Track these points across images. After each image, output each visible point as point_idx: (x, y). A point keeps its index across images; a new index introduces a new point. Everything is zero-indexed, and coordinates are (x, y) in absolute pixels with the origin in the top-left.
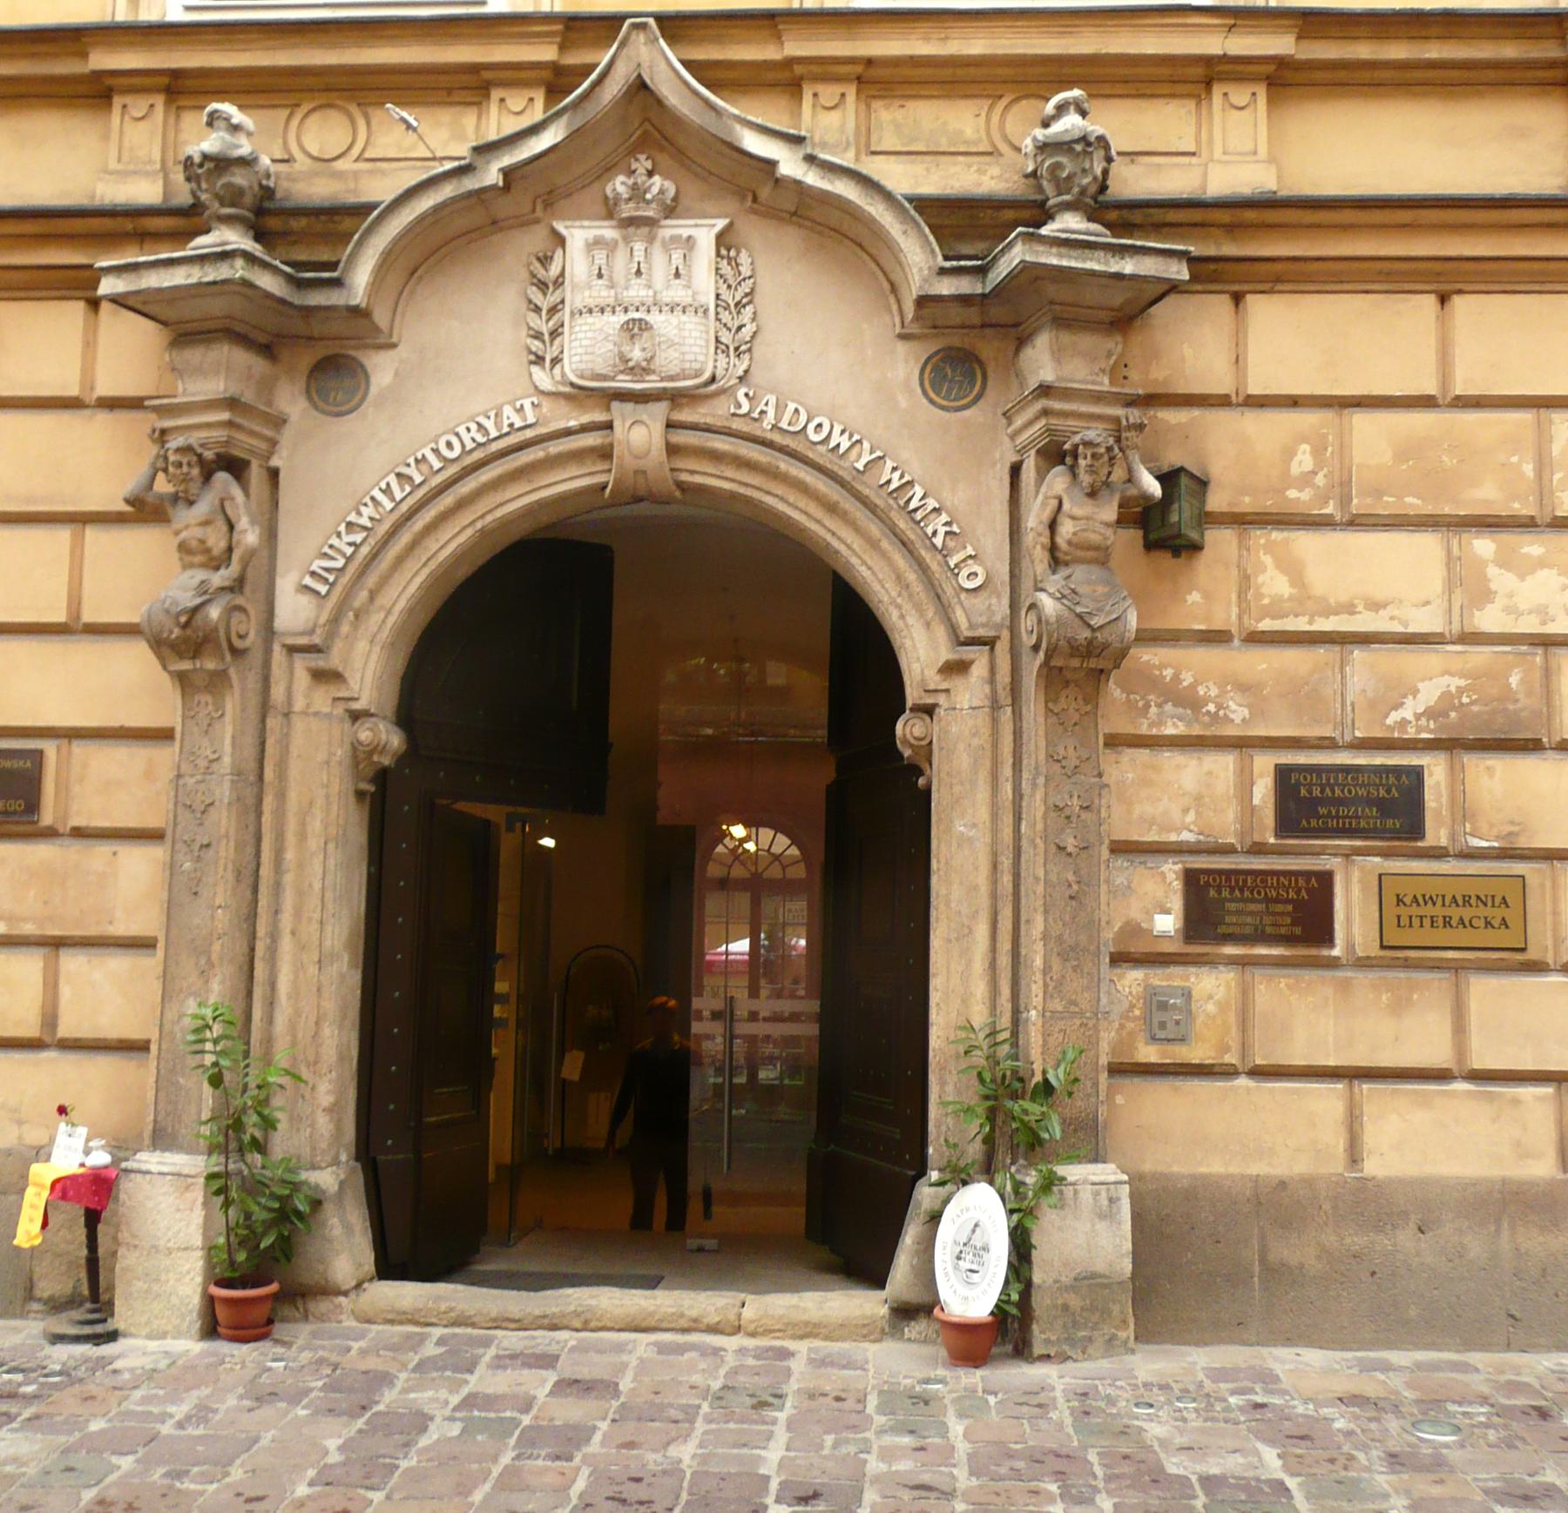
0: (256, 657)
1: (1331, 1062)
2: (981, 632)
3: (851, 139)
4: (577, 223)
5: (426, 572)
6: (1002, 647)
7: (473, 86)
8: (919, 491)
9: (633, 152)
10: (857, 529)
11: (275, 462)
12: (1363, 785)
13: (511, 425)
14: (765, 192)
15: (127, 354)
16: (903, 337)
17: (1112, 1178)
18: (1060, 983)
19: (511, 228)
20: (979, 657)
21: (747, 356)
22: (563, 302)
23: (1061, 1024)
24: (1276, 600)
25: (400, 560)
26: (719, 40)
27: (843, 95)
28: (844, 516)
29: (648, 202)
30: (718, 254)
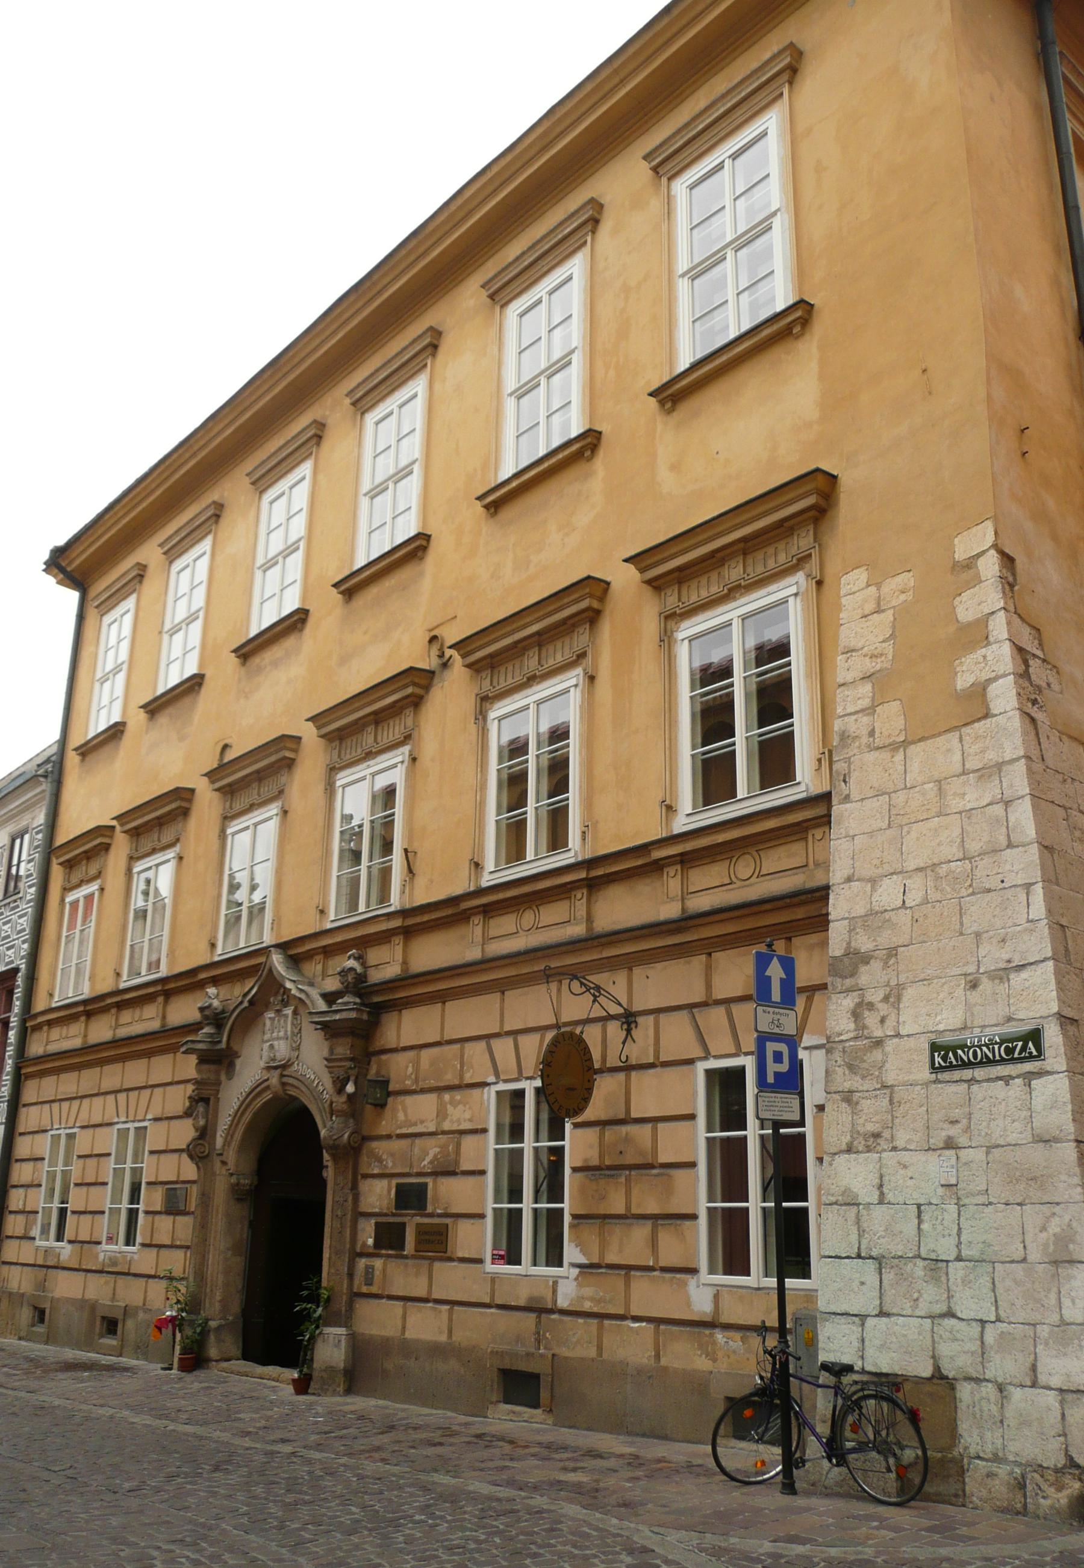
1: (401, 1294)
26: (296, 947)
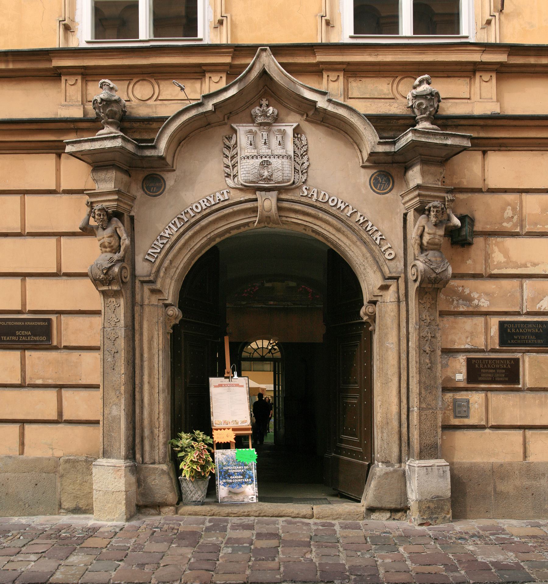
0: (129, 286)
1: (519, 424)
2: (394, 275)
3: (342, 93)
4: (241, 125)
5: (190, 253)
6: (401, 281)
7: (199, 72)
8: (370, 224)
9: (261, 98)
10: (348, 238)
11: (132, 213)
12: (530, 328)
13: (219, 200)
14: (311, 113)
15: (75, 174)
16: (363, 167)
17: (444, 464)
18: (424, 399)
19: (215, 126)
20: (393, 283)
21: (306, 174)
22: (237, 154)
23: (425, 412)
24: (499, 263)
25: (181, 249)
26: (292, 55)
27: (338, 76)
28: (343, 233)
29: (268, 117)
30: (294, 136)
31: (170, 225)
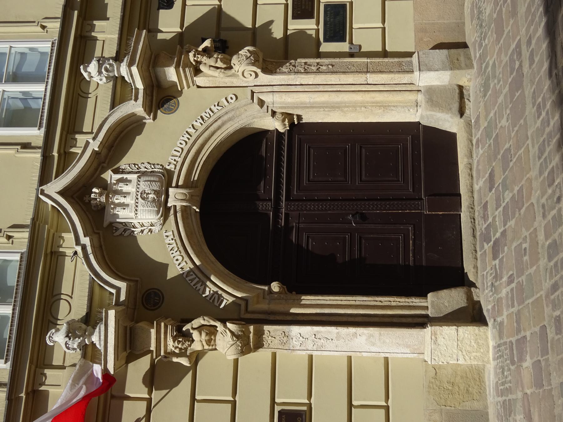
6: (256, 89)
31: (192, 284)
